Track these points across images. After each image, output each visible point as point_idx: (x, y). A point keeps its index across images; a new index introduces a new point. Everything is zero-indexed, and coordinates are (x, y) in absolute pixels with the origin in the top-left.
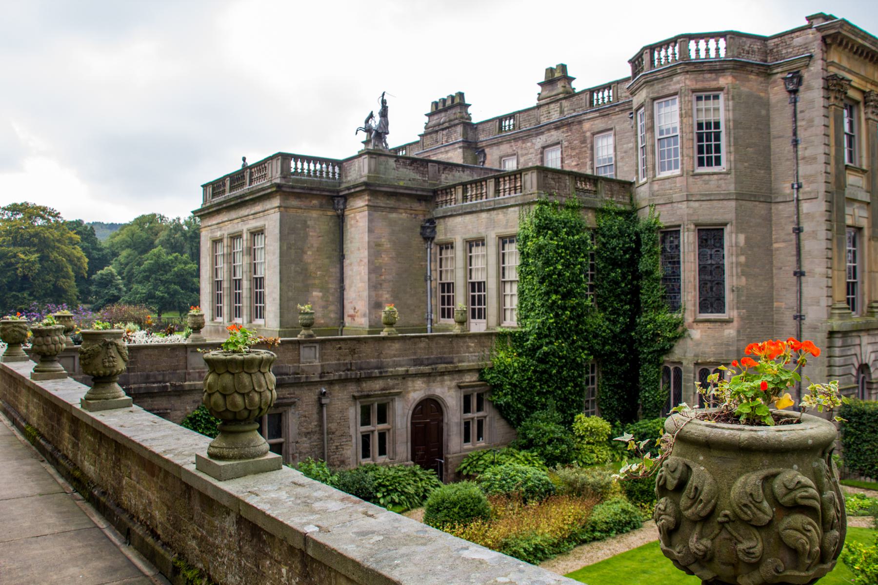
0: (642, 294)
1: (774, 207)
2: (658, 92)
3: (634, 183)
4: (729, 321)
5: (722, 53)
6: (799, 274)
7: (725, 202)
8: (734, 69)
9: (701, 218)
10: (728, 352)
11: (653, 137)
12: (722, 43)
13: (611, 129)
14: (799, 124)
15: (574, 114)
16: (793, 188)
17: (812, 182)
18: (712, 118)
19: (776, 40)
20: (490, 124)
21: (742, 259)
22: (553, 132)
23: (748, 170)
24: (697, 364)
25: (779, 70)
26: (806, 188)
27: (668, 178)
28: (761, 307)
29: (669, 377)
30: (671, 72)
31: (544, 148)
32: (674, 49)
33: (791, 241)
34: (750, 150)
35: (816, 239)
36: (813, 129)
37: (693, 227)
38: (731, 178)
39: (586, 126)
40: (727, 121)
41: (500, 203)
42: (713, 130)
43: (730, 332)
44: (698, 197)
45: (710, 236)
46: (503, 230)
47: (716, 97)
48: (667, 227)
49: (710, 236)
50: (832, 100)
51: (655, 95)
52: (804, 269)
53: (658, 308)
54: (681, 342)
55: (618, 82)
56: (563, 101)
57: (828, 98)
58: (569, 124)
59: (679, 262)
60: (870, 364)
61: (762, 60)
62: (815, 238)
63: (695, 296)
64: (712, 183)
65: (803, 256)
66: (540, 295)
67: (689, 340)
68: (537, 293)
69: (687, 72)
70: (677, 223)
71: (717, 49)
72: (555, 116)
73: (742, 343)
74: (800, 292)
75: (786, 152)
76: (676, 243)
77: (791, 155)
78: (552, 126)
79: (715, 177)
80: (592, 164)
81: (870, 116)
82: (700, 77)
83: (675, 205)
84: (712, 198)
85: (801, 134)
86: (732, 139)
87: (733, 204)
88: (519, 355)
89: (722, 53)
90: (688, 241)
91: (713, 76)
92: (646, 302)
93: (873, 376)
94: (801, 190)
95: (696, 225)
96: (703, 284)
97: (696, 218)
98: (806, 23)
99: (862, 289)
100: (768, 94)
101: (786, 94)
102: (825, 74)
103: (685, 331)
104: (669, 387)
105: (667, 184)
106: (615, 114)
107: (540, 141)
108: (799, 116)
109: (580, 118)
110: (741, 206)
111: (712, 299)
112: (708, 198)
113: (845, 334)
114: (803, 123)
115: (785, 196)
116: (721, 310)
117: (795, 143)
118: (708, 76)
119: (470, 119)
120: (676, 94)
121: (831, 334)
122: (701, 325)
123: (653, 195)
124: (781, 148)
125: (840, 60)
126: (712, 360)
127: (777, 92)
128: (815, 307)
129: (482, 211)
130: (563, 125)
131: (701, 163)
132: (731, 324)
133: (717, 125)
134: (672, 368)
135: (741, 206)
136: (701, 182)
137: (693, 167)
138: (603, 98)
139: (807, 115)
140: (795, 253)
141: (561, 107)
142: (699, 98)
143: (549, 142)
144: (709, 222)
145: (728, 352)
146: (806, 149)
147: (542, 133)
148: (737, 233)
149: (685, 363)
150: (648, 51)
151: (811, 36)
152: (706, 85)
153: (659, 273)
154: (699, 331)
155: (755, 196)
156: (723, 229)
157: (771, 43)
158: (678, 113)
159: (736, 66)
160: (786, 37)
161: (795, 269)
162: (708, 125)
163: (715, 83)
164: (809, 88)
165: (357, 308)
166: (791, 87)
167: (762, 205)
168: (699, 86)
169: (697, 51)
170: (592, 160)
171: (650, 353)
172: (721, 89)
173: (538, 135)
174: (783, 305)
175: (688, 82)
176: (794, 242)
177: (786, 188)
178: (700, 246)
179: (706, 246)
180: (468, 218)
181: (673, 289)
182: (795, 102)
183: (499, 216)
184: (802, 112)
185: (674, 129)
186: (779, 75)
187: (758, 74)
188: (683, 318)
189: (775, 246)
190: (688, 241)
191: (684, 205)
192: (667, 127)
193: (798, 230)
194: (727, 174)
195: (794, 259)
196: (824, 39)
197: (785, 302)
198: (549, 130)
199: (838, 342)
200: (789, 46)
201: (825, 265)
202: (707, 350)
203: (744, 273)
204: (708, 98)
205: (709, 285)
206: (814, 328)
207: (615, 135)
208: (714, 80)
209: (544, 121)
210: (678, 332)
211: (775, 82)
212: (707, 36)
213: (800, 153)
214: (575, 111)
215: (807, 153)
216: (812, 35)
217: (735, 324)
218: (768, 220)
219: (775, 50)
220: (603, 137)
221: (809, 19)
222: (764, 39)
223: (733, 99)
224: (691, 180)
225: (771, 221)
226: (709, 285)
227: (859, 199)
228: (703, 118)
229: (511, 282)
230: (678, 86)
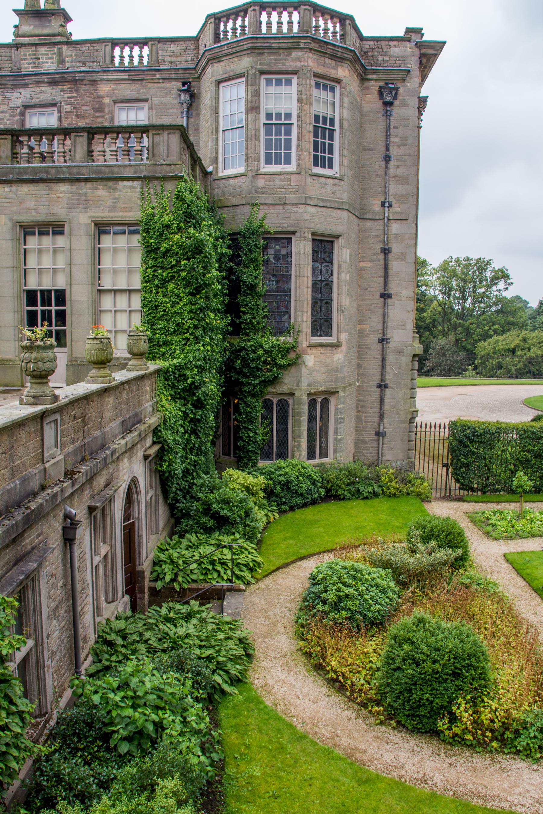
0: (244, 313)
2: (269, 65)
3: (211, 173)
6: (385, 296)
7: (339, 211)
8: (351, 62)
9: (317, 226)
10: (337, 379)
11: (256, 120)
13: (146, 100)
14: (392, 139)
15: (83, 69)
16: (383, 204)
17: (402, 203)
19: (372, 43)
22: (45, 88)
25: (375, 77)
26: (396, 208)
27: (280, 174)
29: (272, 411)
30: (291, 44)
31: (26, 107)
32: (243, 21)
33: (379, 261)
35: (405, 261)
36: (407, 147)
37: (310, 236)
39: (104, 89)
41: (100, 172)
42: (328, 127)
43: (339, 357)
46: (107, 214)
47: (333, 89)
48: (276, 233)
51: (265, 68)
52: (391, 291)
54: (293, 370)
55: (160, 40)
56: (65, 47)
58: (74, 81)
59: (288, 277)
62: (403, 260)
64: (328, 187)
65: (390, 278)
66: (191, 311)
67: (303, 367)
68: (187, 308)
70: (292, 229)
72: (49, 65)
74: (384, 315)
75: (377, 167)
76: (283, 252)
77: (381, 171)
78: (45, 78)
79: (331, 181)
83: (289, 207)
84: (328, 205)
85: (394, 151)
87: (345, 214)
88: (173, 398)
90: (302, 251)
92: (251, 323)
94: (391, 209)
95: (313, 234)
96: (315, 301)
97: (312, 225)
101: (379, 104)
103: (298, 357)
104: (271, 423)
105: (278, 181)
106: (153, 81)
107: (19, 97)
108: (392, 131)
109: (95, 77)
114: (397, 140)
115: (374, 213)
116: (328, 333)
117: (387, 159)
118: (328, 61)
120: (295, 73)
122: (314, 350)
123: (257, 192)
126: (323, 389)
127: (372, 101)
128: (400, 331)
129: (61, 180)
130: (64, 81)
131: (316, 164)
133: (332, 121)
134: (275, 401)
136: (318, 185)
138: (131, 57)
139: (401, 132)
140: (383, 274)
141: (60, 54)
143: (36, 101)
145: (337, 379)
146: (398, 167)
147: (25, 86)
149: (297, 394)
150: (257, 8)
151: (409, 50)
153: (261, 289)
154: (313, 356)
156: (332, 242)
157: (367, 45)
158: (295, 97)
160: (383, 43)
161: (382, 291)
162: (325, 118)
163: (334, 72)
166: (389, 99)
168: (320, 70)
172: (338, 81)
173: (15, 87)
174: (367, 328)
176: (382, 263)
178: (314, 260)
180: (25, 189)
181: (278, 308)
182: (388, 115)
183: (101, 191)
184: (394, 127)
185: (288, 116)
186: (372, 83)
188: (296, 342)
190: (302, 251)
192: (279, 111)
193: (386, 251)
195: (382, 280)
196: (421, 56)
198: (38, 83)
200: (385, 54)
202: (319, 378)
204: (325, 87)
206: (399, 352)
207: (151, 109)
208: (334, 68)
209: (27, 67)
210: (290, 358)
211: (368, 88)
214: (84, 64)
215: (399, 172)
217: (344, 348)
219: (370, 54)
220: (132, 108)
224: (309, 180)
229: (115, 291)
230: (299, 64)
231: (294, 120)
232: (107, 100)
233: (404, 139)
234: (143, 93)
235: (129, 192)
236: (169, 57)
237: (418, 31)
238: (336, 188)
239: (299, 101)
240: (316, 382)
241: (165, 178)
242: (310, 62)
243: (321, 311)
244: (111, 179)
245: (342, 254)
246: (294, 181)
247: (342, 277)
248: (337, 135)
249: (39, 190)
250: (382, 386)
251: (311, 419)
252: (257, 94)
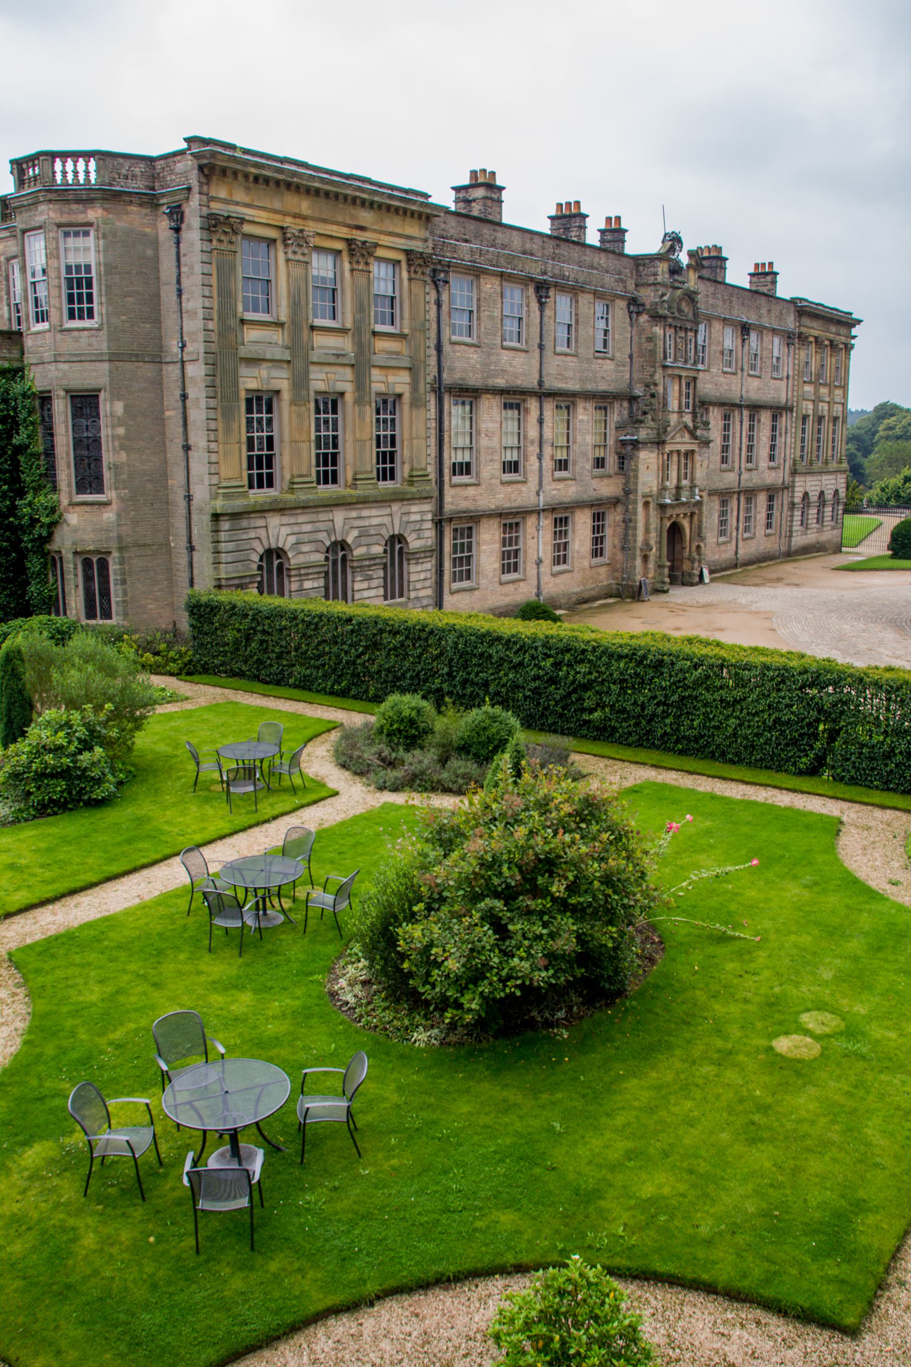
1: (164, 367)
4: (107, 504)
5: (93, 177)
7: (98, 364)
8: (103, 199)
10: (108, 539)
12: (92, 165)
14: (183, 269)
18: (81, 260)
21: (121, 431)
23: (128, 325)
24: (76, 553)
26: (190, 348)
28: (150, 486)
34: (131, 300)
37: (62, 393)
38: (103, 334)
40: (99, 264)
43: (109, 515)
44: (67, 358)
45: (85, 403)
49: (85, 403)
50: (215, 242)
53: (37, 490)
54: (59, 527)
57: (211, 241)
60: (286, 548)
61: (147, 187)
62: (198, 407)
63: (69, 475)
64: (83, 340)
67: (65, 526)
69: (50, 201)
70: (48, 388)
71: (87, 173)
73: (124, 528)
77: (175, 307)
79: (86, 333)
80: (9, 299)
81: (291, 256)
82: (66, 208)
86: (103, 288)
87: (106, 366)
89: (93, 177)
90: (61, 409)
91: (81, 207)
93: (292, 562)
95: (67, 391)
96: (79, 461)
97: (65, 382)
98: (184, 145)
99: (281, 462)
100: (157, 229)
102: (205, 211)
108: (182, 259)
110: (117, 368)
111: (90, 478)
112: (78, 359)
113: (235, 516)
116: (100, 491)
118: (74, 207)
120: (40, 228)
121: (216, 517)
122: (77, 509)
124: (168, 294)
125: (231, 194)
126: (92, 548)
131: (72, 316)
132: (110, 508)
133: (88, 268)
135: (117, 368)
137: (61, 321)
142: (67, 235)
144: (80, 387)
145: (108, 539)
148: (112, 401)
149: (64, 551)
152: (73, 218)
155: (137, 356)
159: (109, 196)
160: (170, 160)
162: (78, 267)
163: (82, 216)
164: (189, 227)
167: (147, 366)
168: (65, 219)
169: (64, 173)
170: (8, 293)
171: (31, 541)
175: (52, 214)
177: (174, 345)
178: (74, 416)
179: (82, 416)
187: (141, 205)
188: (59, 501)
189: (167, 413)
190: (61, 409)
191: (52, 367)
193: (184, 397)
194: (98, 330)
195: (181, 430)
196: (201, 168)
197: (176, 480)
199: (225, 525)
201: (206, 439)
202: (86, 537)
203: (123, 447)
204: (77, 234)
205: (86, 461)
208: (82, 212)
212: (76, 155)
216: (187, 165)
217: (114, 506)
218: (158, 383)
221: (188, 140)
222: (150, 160)
223: (105, 236)
224: (59, 336)
225: (161, 384)
226: (86, 461)
227: (268, 357)
228: (72, 260)
238: (93, 339)
240: (82, 540)
242: (46, 213)
243: (89, 468)
245: (110, 408)
247: (109, 432)
250: (191, 549)
251: (88, 579)
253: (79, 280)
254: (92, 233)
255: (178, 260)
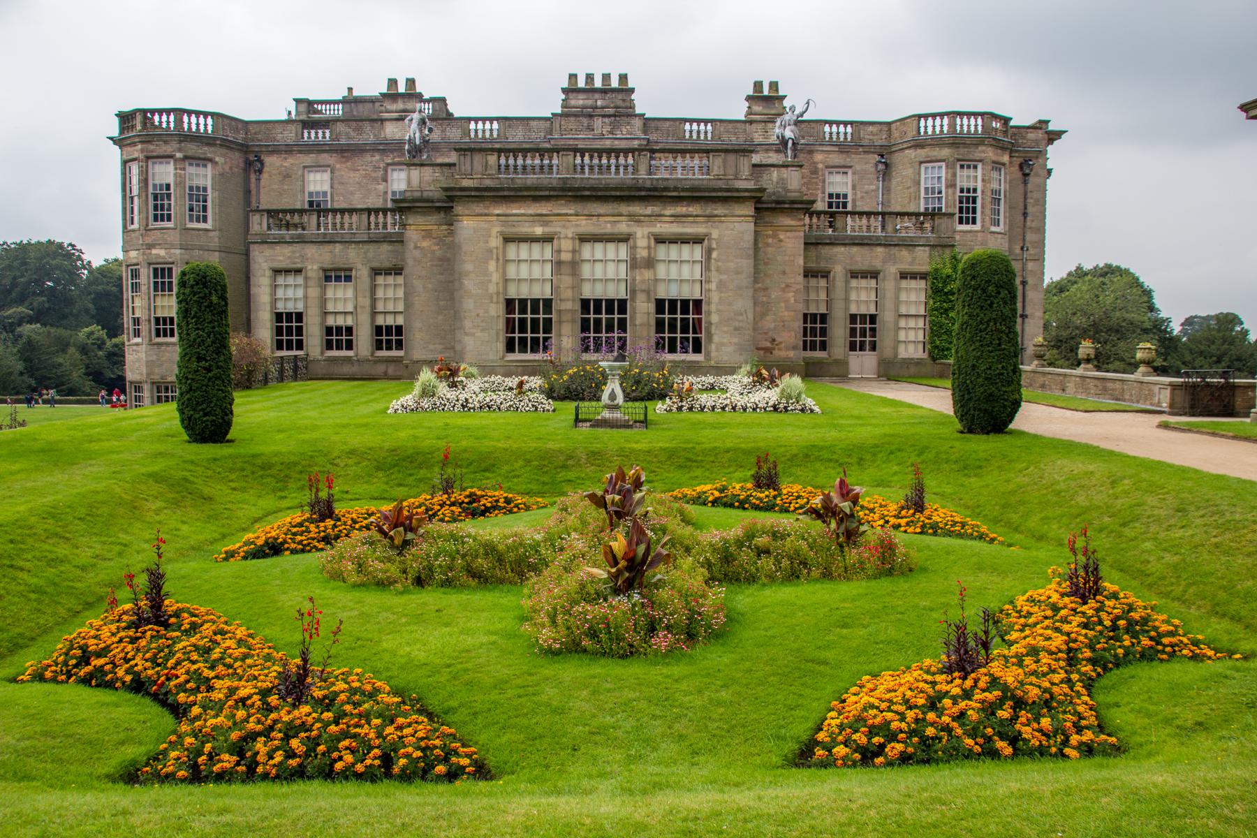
16: (1022, 248)
20: (668, 124)
26: (1032, 251)
27: (970, 232)
30: (977, 141)
39: (819, 157)
85: (1030, 209)
101: (1019, 175)
106: (856, 153)
108: (1029, 195)
109: (812, 148)
117: (1025, 215)
119: (633, 107)
165: (779, 339)
168: (994, 158)
180: (855, 249)
182: (1025, 183)
183: (905, 253)
198: (767, 151)
200: (1024, 138)
207: (854, 173)
213: (1028, 223)
215: (1033, 225)
230: (983, 155)
231: (979, 193)
232: (820, 166)
233: (1037, 201)
234: (848, 161)
235: (922, 254)
236: (866, 135)
237: (1047, 122)
239: (983, 180)
241: (946, 246)
242: (989, 153)
244: (910, 245)
246: (980, 237)
248: (1002, 202)
249: (864, 250)
252: (954, 175)
253: (968, 198)
254: (980, 166)
255: (1025, 194)
